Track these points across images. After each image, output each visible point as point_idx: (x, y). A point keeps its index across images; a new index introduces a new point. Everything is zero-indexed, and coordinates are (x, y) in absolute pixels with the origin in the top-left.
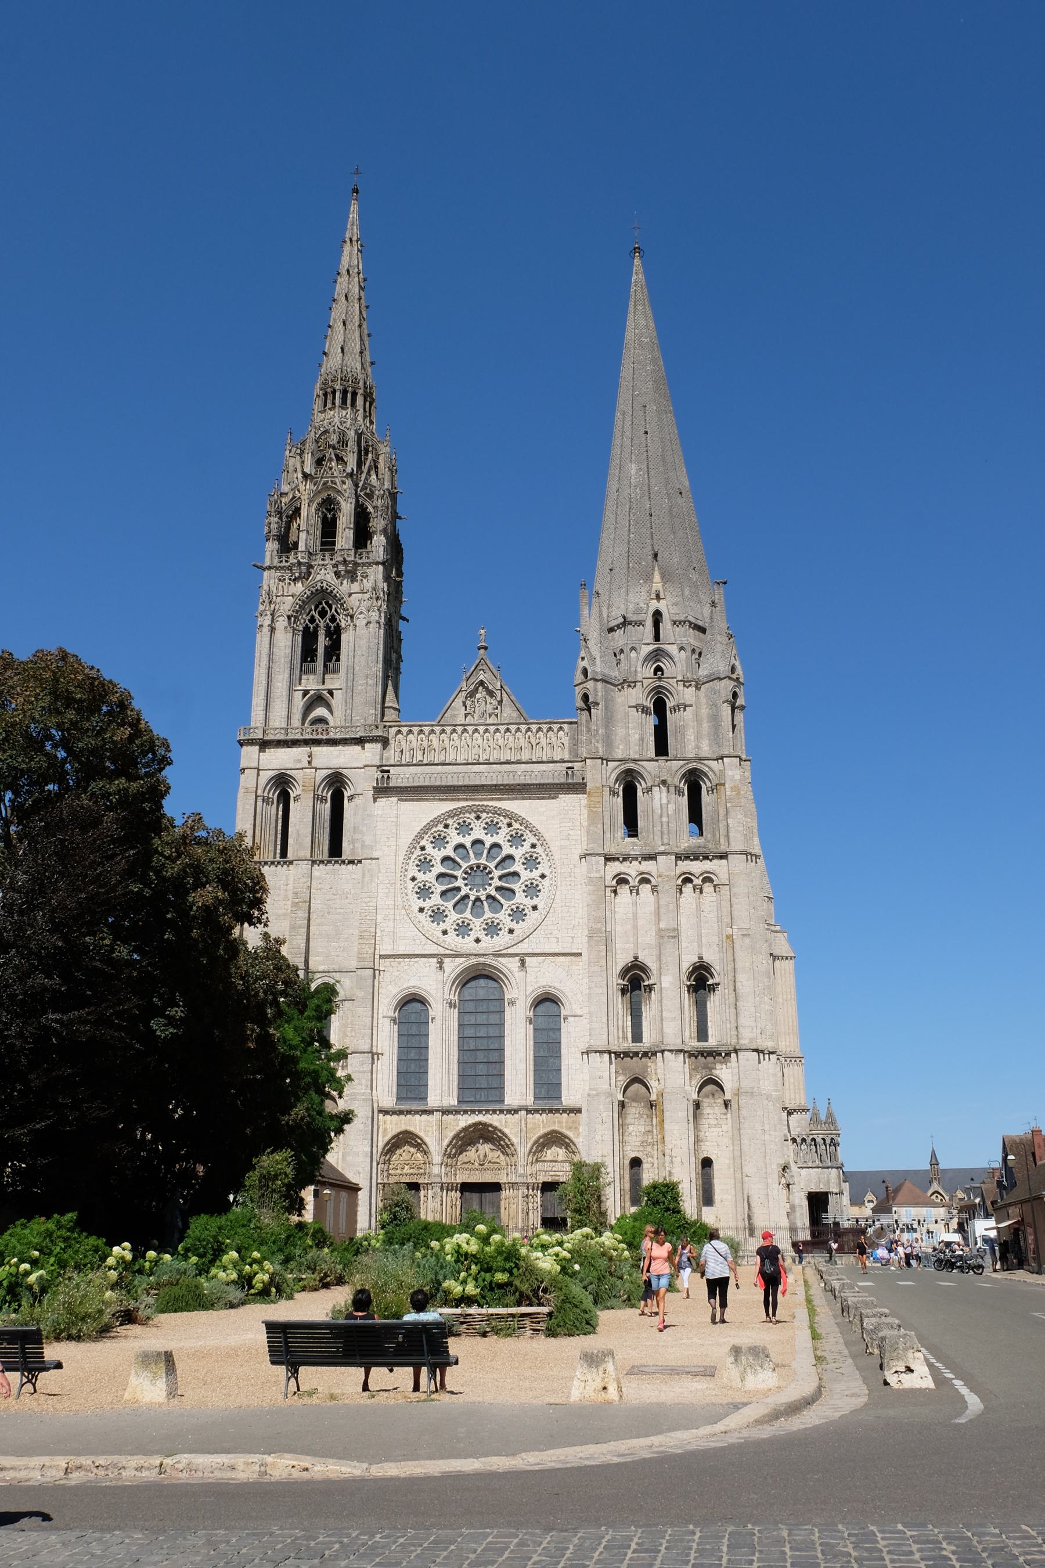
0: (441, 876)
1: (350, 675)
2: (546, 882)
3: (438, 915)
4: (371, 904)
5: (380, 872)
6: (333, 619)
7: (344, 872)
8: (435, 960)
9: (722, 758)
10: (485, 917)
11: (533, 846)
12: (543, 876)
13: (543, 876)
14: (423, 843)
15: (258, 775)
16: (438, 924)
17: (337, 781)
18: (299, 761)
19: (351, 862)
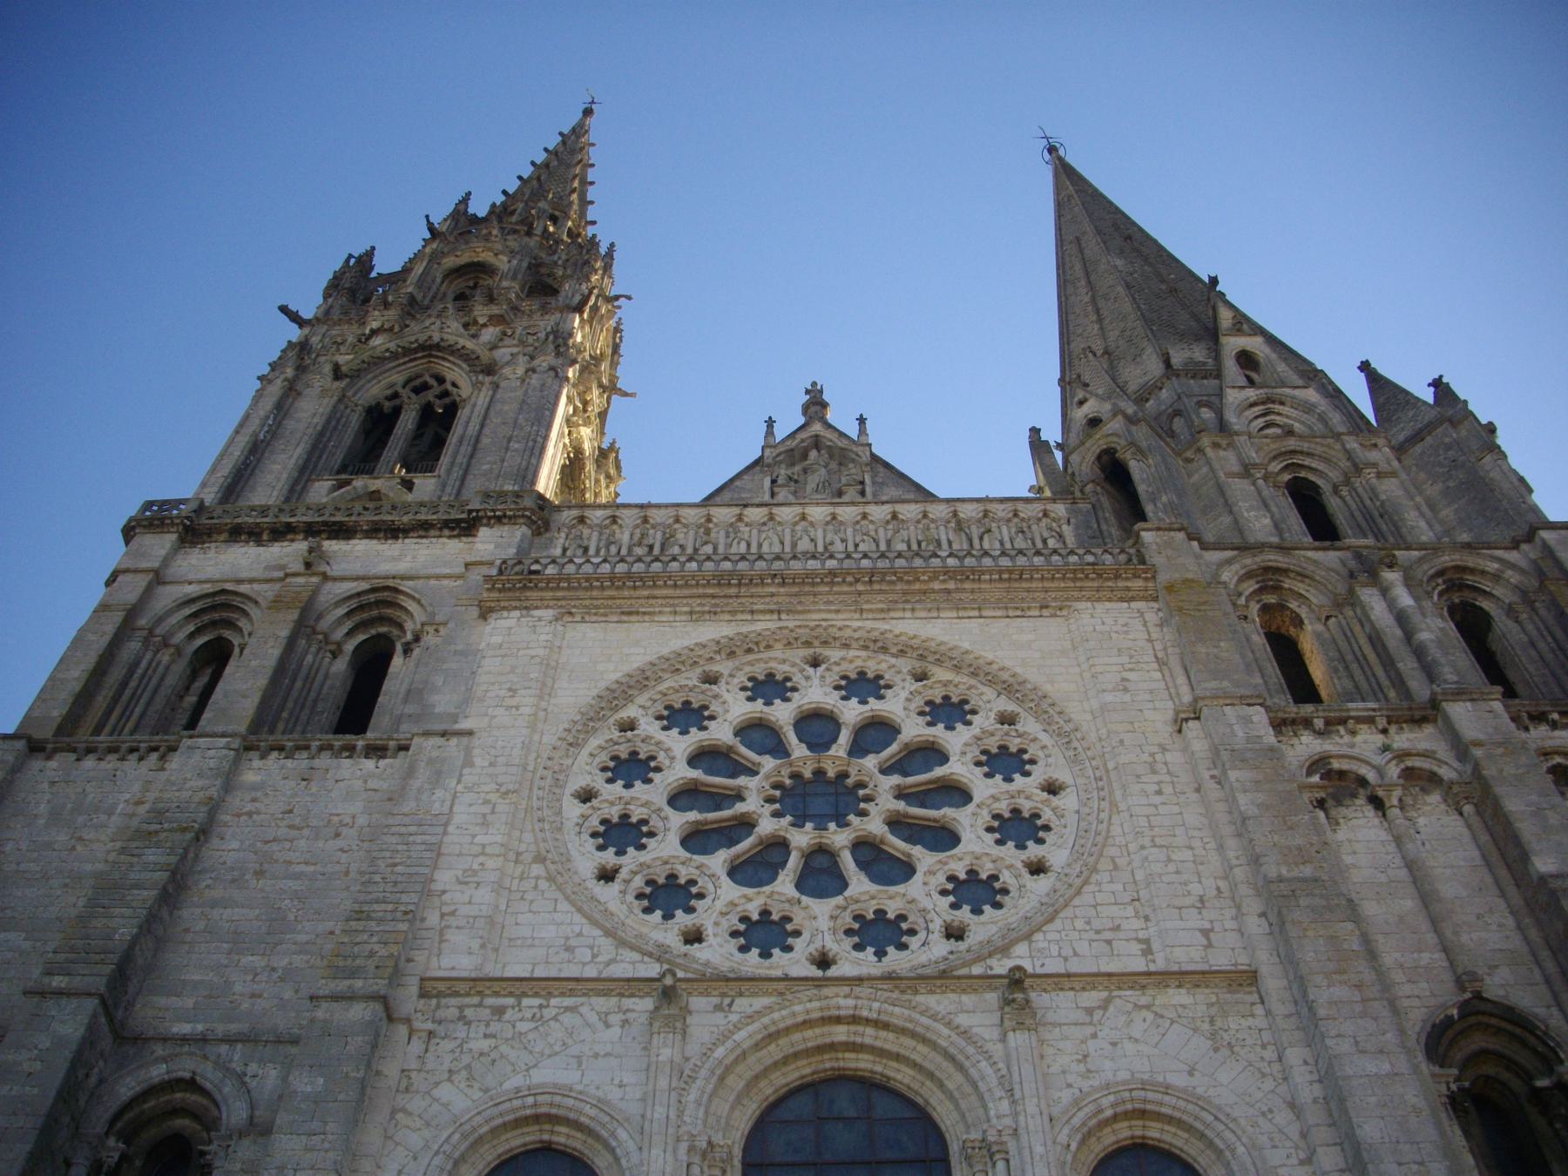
0: (683, 797)
1: (465, 449)
2: (1068, 801)
3: (668, 895)
4: (419, 839)
5: (472, 765)
6: (446, 394)
7: (346, 774)
8: (648, 1004)
9: (1530, 537)
10: (847, 893)
11: (1007, 719)
12: (1052, 789)
13: (1052, 789)
14: (631, 712)
15: (148, 592)
16: (668, 916)
17: (382, 619)
18: (281, 567)
19: (377, 751)
